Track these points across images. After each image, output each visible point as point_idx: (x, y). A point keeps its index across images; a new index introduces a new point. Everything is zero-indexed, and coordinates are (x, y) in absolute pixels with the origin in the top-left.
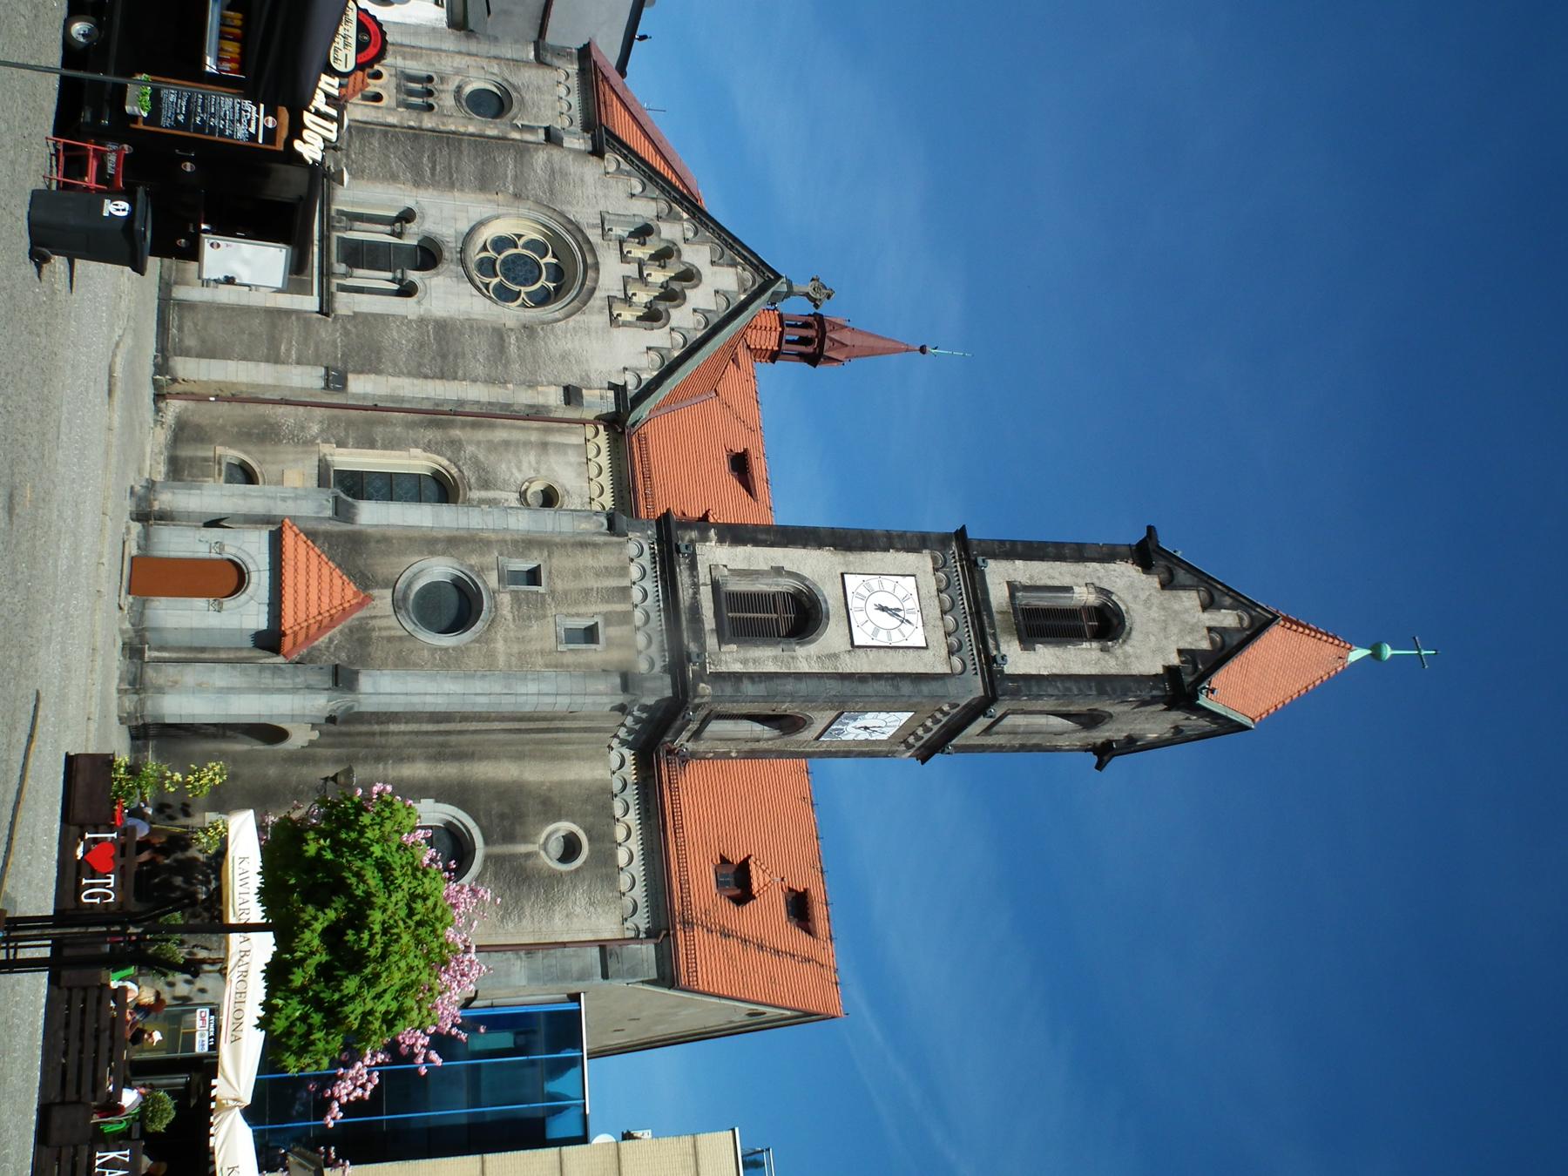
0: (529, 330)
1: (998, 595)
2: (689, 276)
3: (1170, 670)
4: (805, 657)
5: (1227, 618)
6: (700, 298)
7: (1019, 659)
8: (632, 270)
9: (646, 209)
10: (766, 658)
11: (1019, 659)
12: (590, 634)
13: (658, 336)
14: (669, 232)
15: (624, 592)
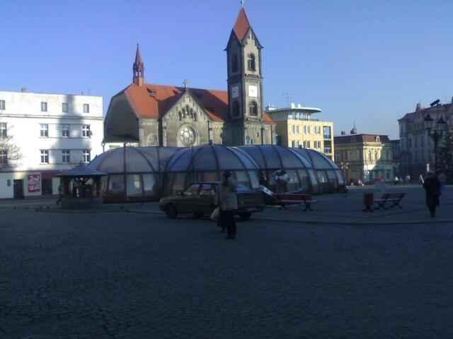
0: (201, 136)
1: (250, 73)
2: (187, 107)
3: (258, 48)
4: (259, 104)
5: (251, 36)
6: (191, 105)
7: (257, 73)
8: (187, 117)
9: (176, 113)
10: (259, 110)
11: (257, 73)
12: (258, 134)
13: (199, 114)
14: (180, 109)
15: (253, 129)
